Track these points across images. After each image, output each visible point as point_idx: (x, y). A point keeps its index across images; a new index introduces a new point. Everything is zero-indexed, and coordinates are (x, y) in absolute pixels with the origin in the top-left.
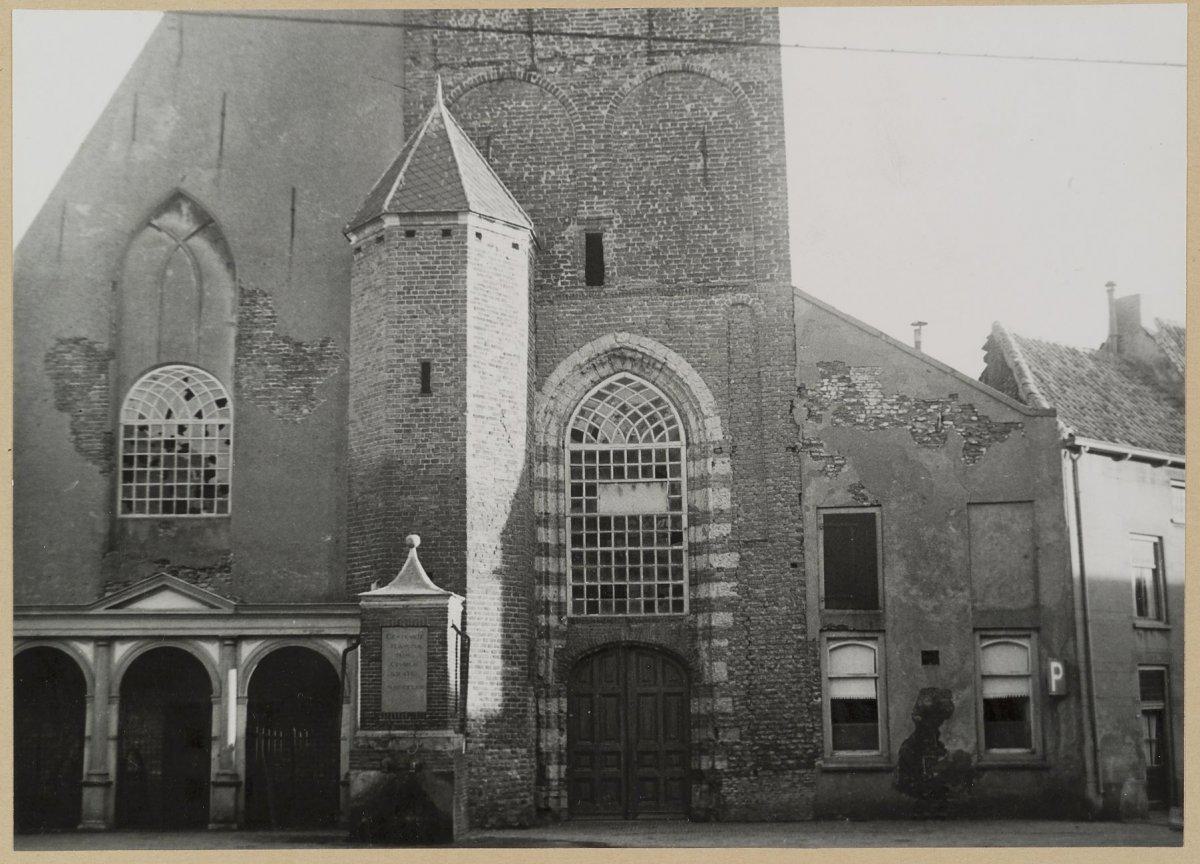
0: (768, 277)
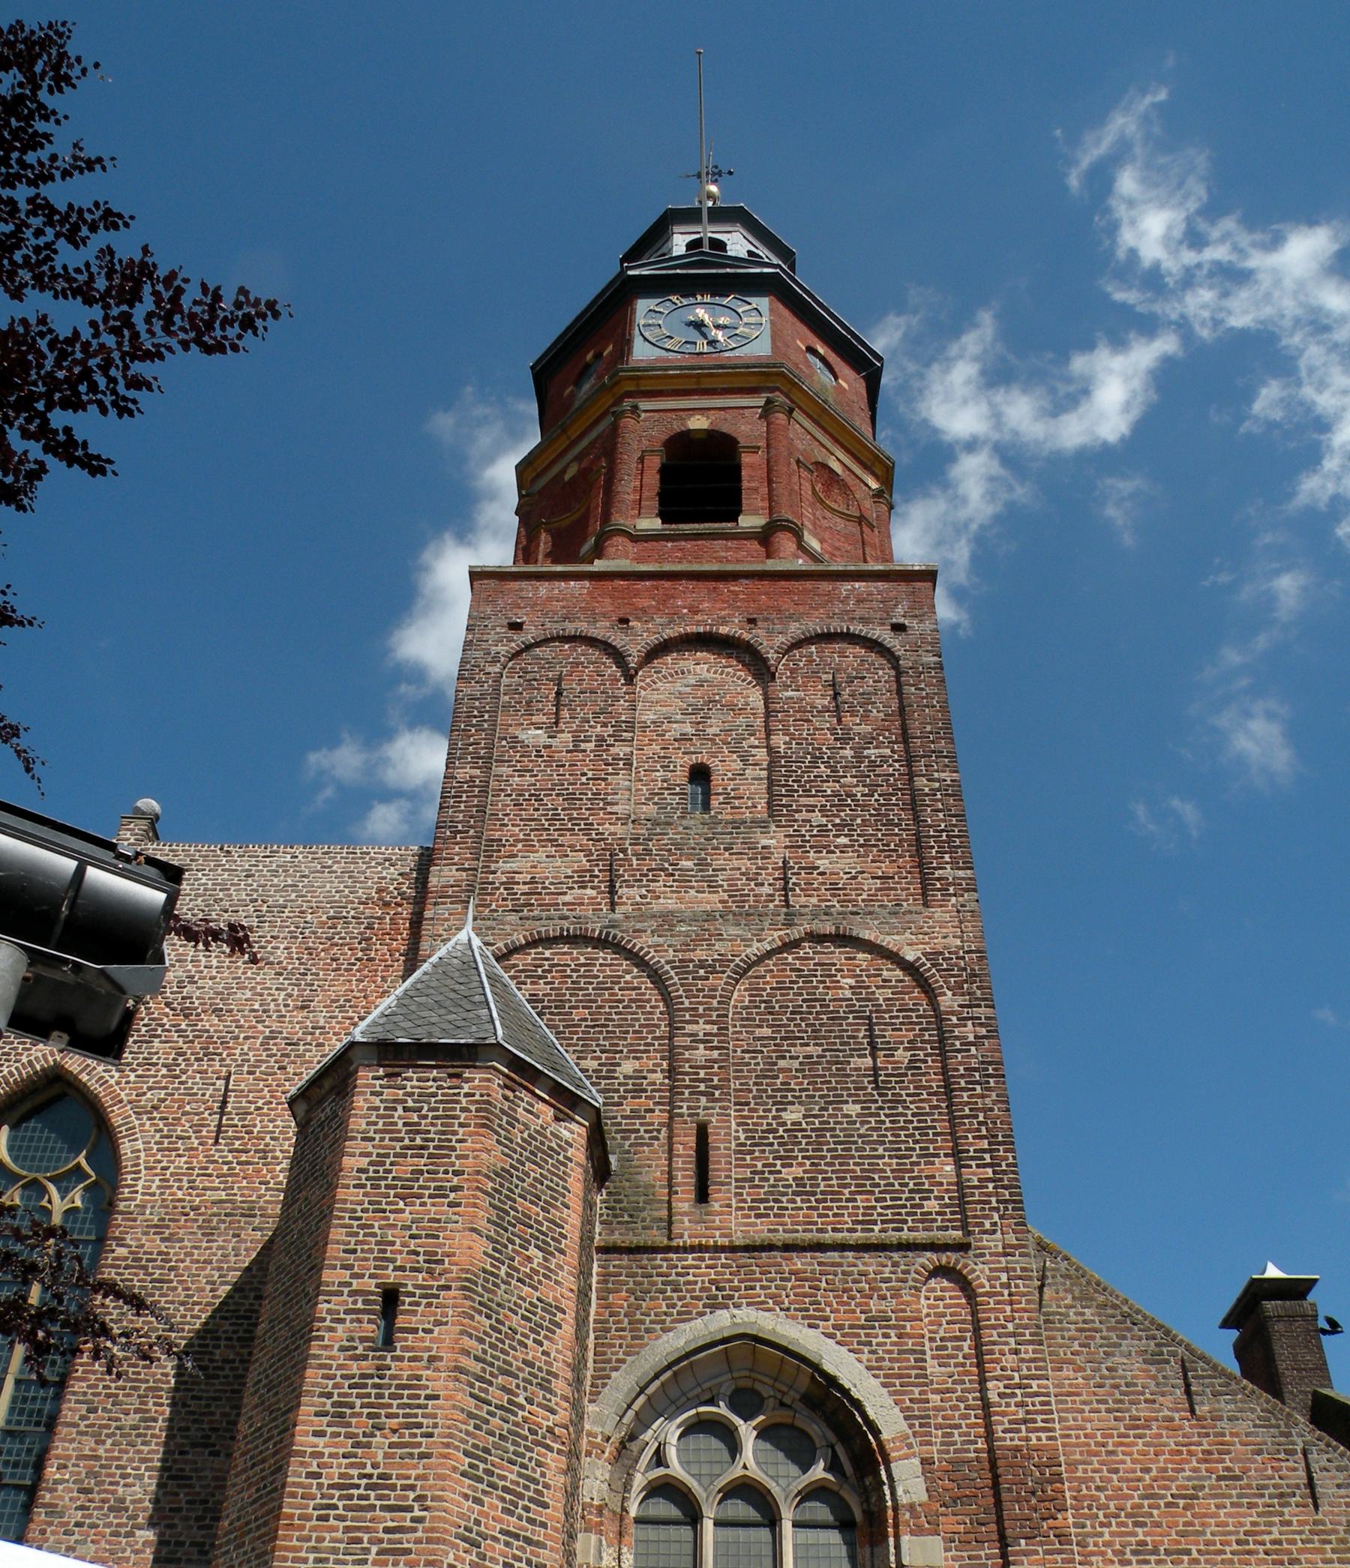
0: (987, 1226)
